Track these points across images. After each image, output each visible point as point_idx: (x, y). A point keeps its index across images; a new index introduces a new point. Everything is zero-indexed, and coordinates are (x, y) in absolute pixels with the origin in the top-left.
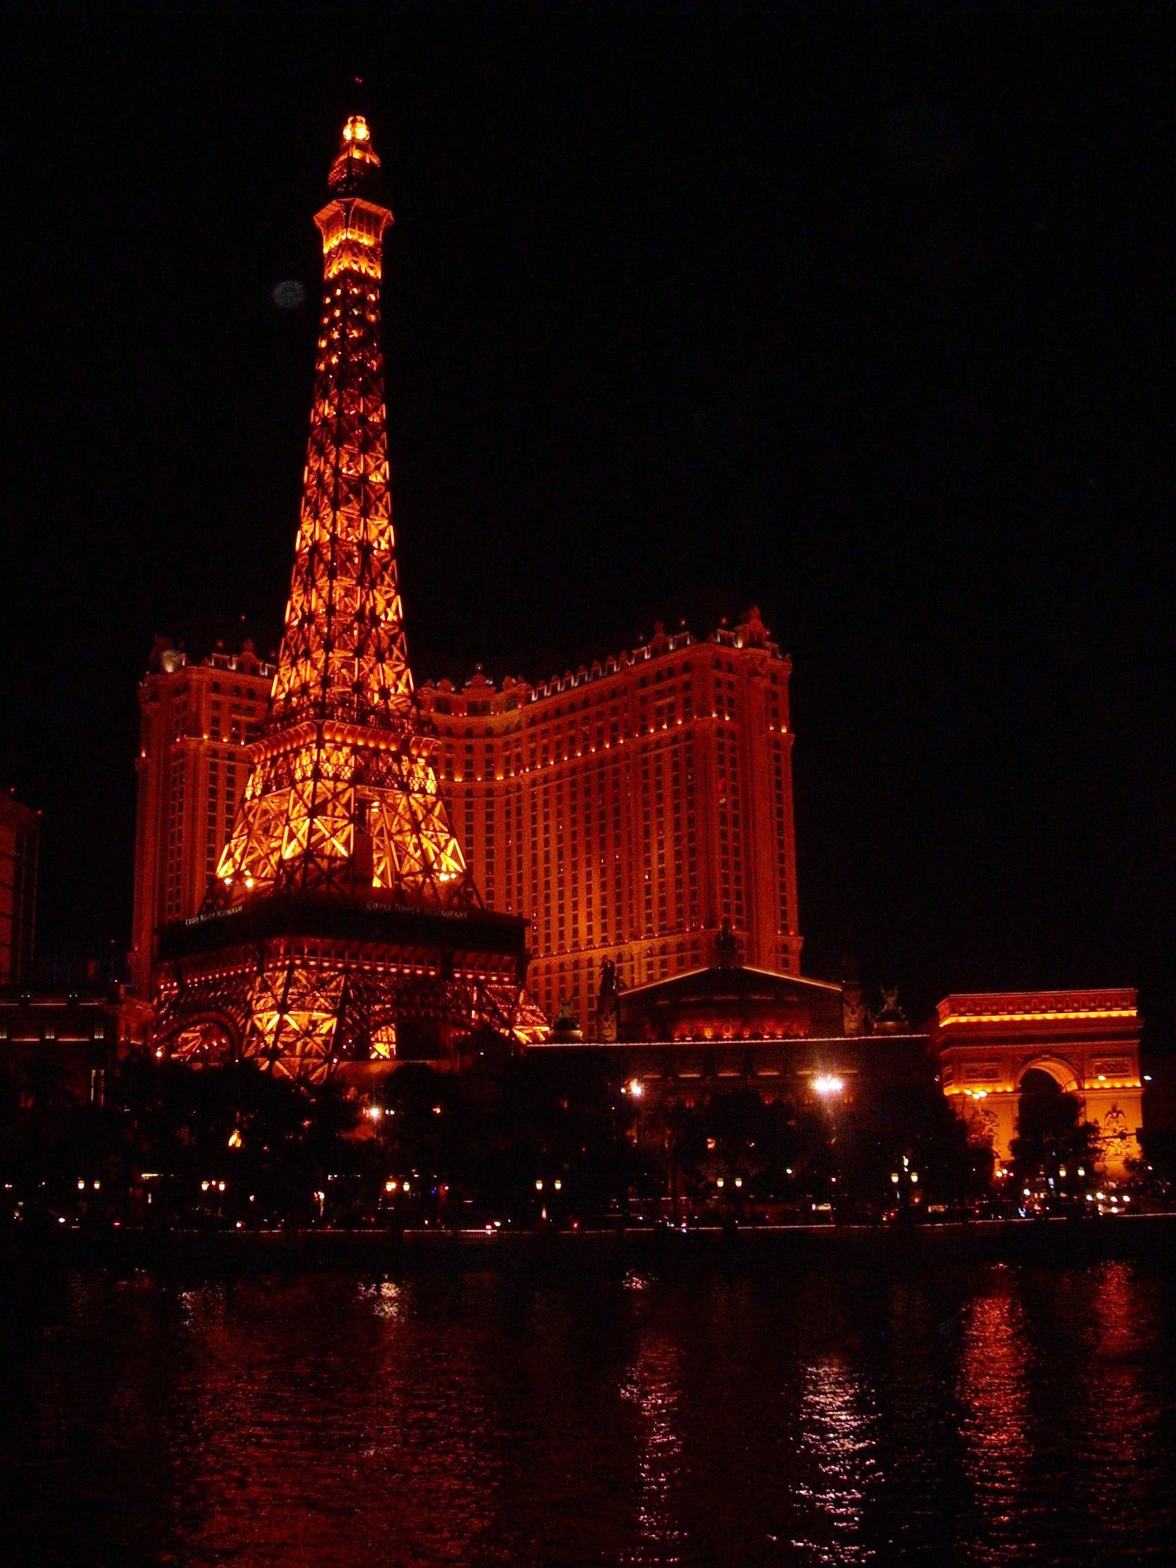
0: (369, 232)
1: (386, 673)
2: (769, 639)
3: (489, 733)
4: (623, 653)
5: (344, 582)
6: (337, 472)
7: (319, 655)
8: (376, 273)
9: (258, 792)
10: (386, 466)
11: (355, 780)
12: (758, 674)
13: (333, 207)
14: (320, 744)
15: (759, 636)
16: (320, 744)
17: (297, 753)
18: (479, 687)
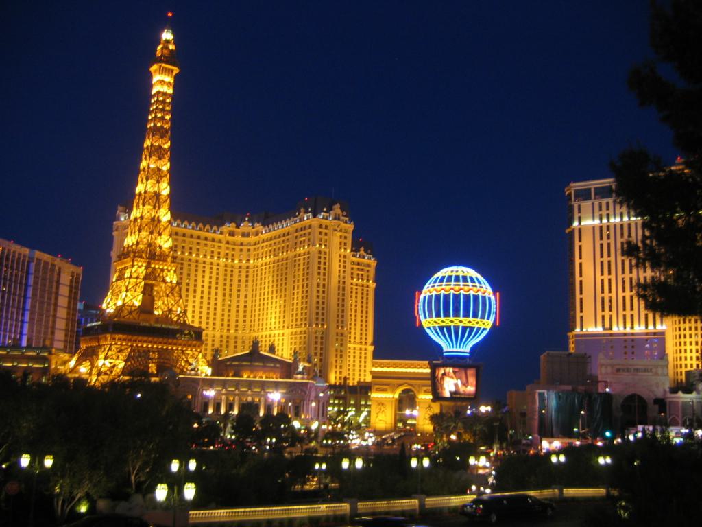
0: (168, 75)
2: (345, 216)
3: (249, 244)
4: (292, 219)
5: (148, 207)
10: (169, 164)
11: (145, 278)
12: (336, 230)
13: (154, 68)
15: (339, 215)
18: (246, 227)
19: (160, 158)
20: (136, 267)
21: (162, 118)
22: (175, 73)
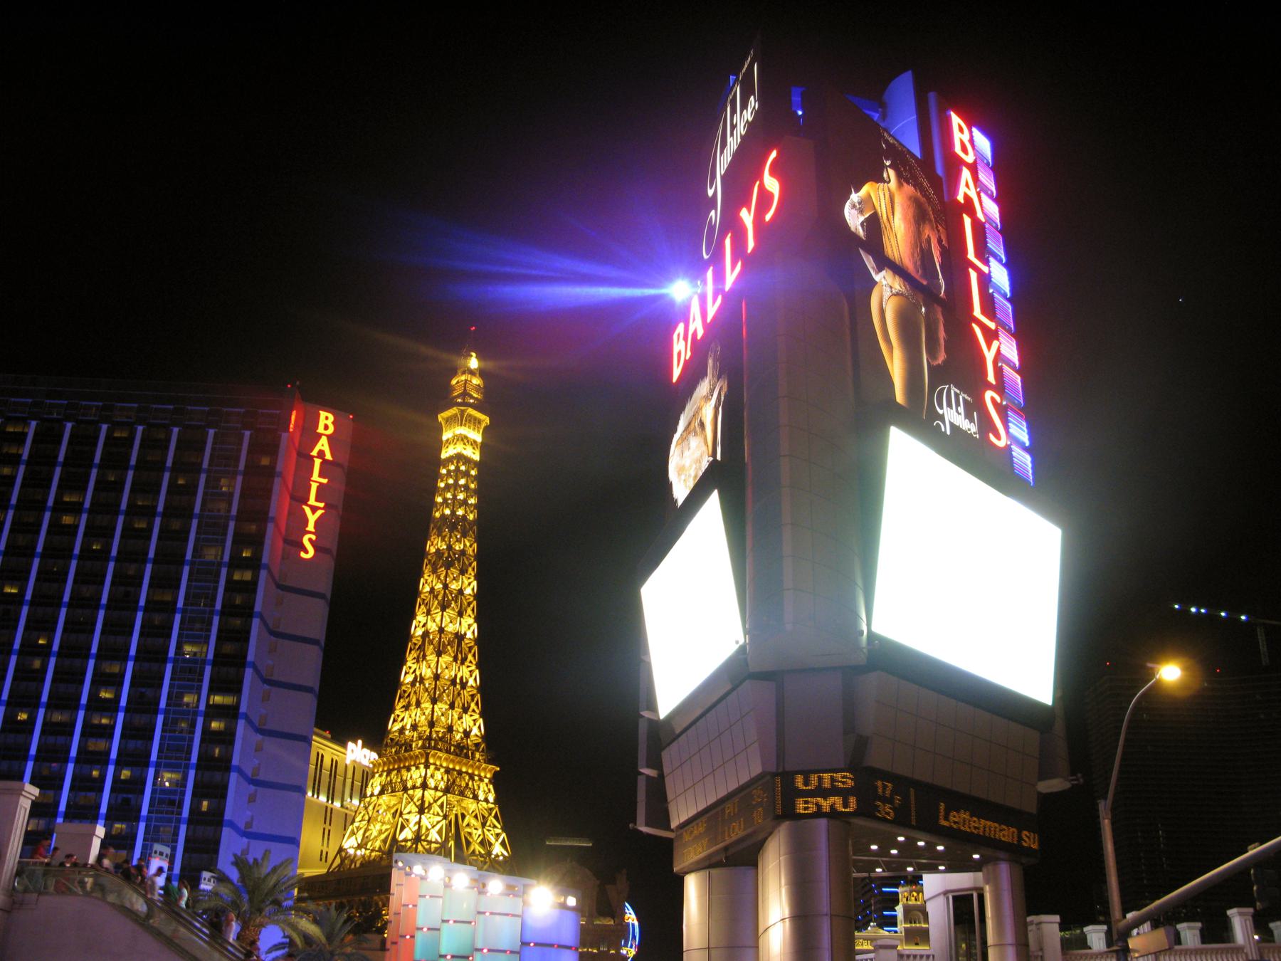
1: (467, 721)
5: (446, 659)
6: (446, 586)
7: (427, 705)
8: (476, 457)
9: (376, 792)
10: (475, 583)
11: (447, 791)
13: (454, 411)
14: (427, 767)
16: (427, 767)
17: (409, 770)
19: (463, 572)
20: (432, 767)
21: (464, 503)
22: (483, 425)
